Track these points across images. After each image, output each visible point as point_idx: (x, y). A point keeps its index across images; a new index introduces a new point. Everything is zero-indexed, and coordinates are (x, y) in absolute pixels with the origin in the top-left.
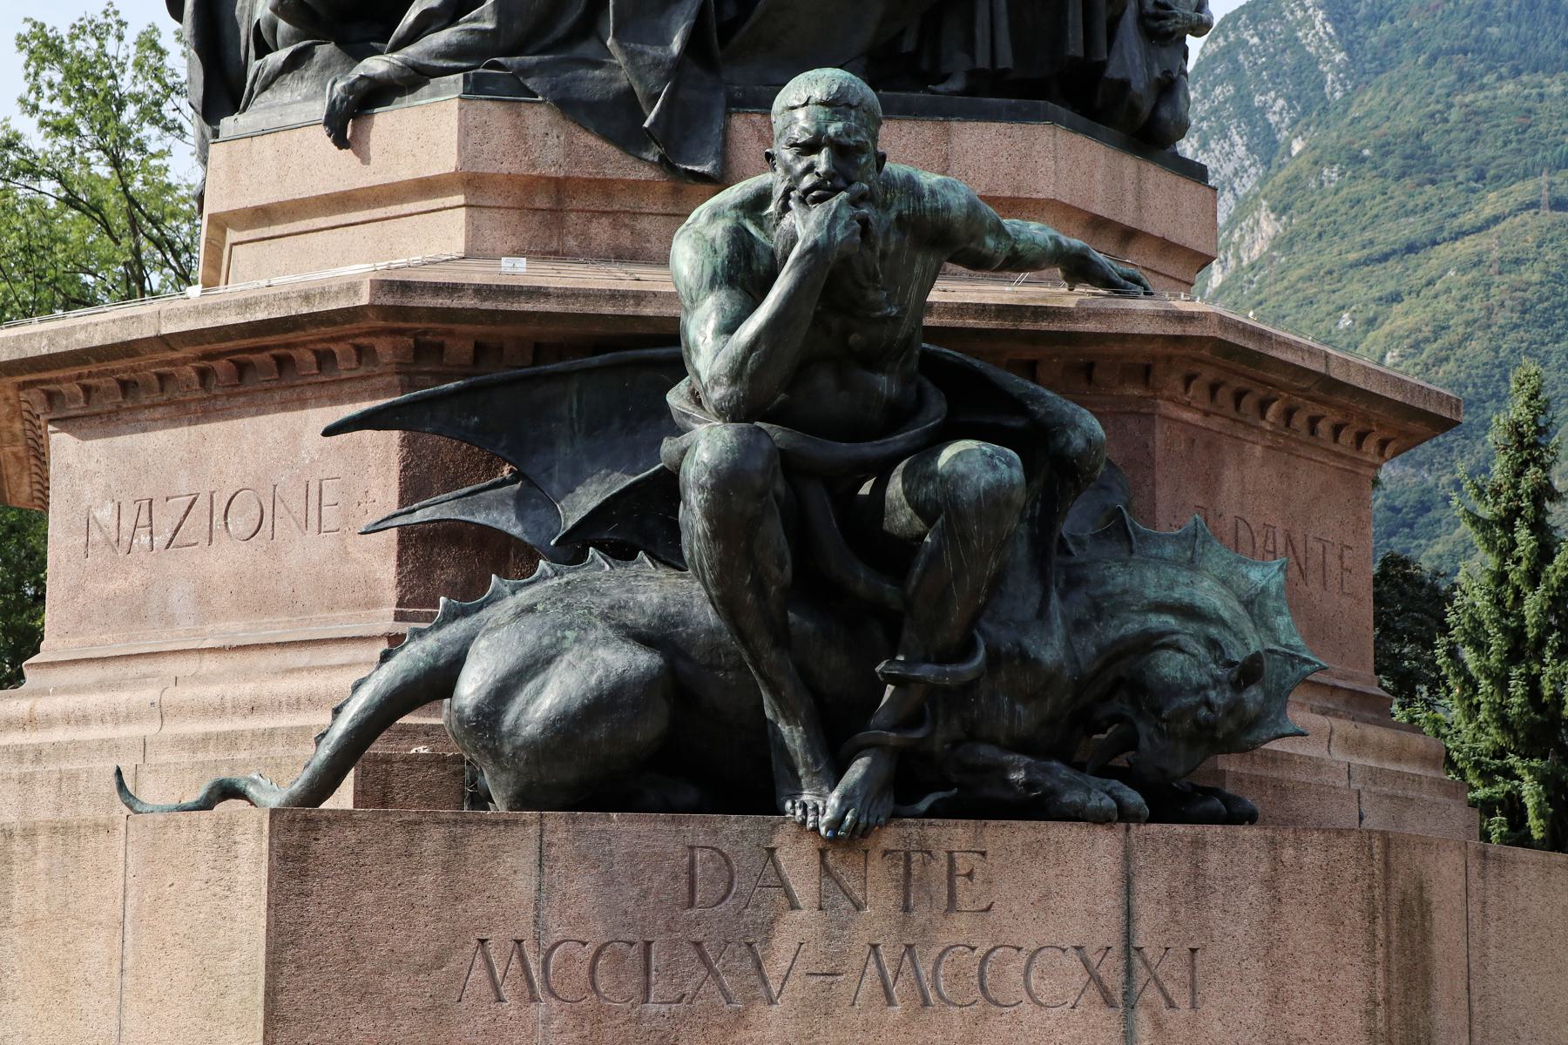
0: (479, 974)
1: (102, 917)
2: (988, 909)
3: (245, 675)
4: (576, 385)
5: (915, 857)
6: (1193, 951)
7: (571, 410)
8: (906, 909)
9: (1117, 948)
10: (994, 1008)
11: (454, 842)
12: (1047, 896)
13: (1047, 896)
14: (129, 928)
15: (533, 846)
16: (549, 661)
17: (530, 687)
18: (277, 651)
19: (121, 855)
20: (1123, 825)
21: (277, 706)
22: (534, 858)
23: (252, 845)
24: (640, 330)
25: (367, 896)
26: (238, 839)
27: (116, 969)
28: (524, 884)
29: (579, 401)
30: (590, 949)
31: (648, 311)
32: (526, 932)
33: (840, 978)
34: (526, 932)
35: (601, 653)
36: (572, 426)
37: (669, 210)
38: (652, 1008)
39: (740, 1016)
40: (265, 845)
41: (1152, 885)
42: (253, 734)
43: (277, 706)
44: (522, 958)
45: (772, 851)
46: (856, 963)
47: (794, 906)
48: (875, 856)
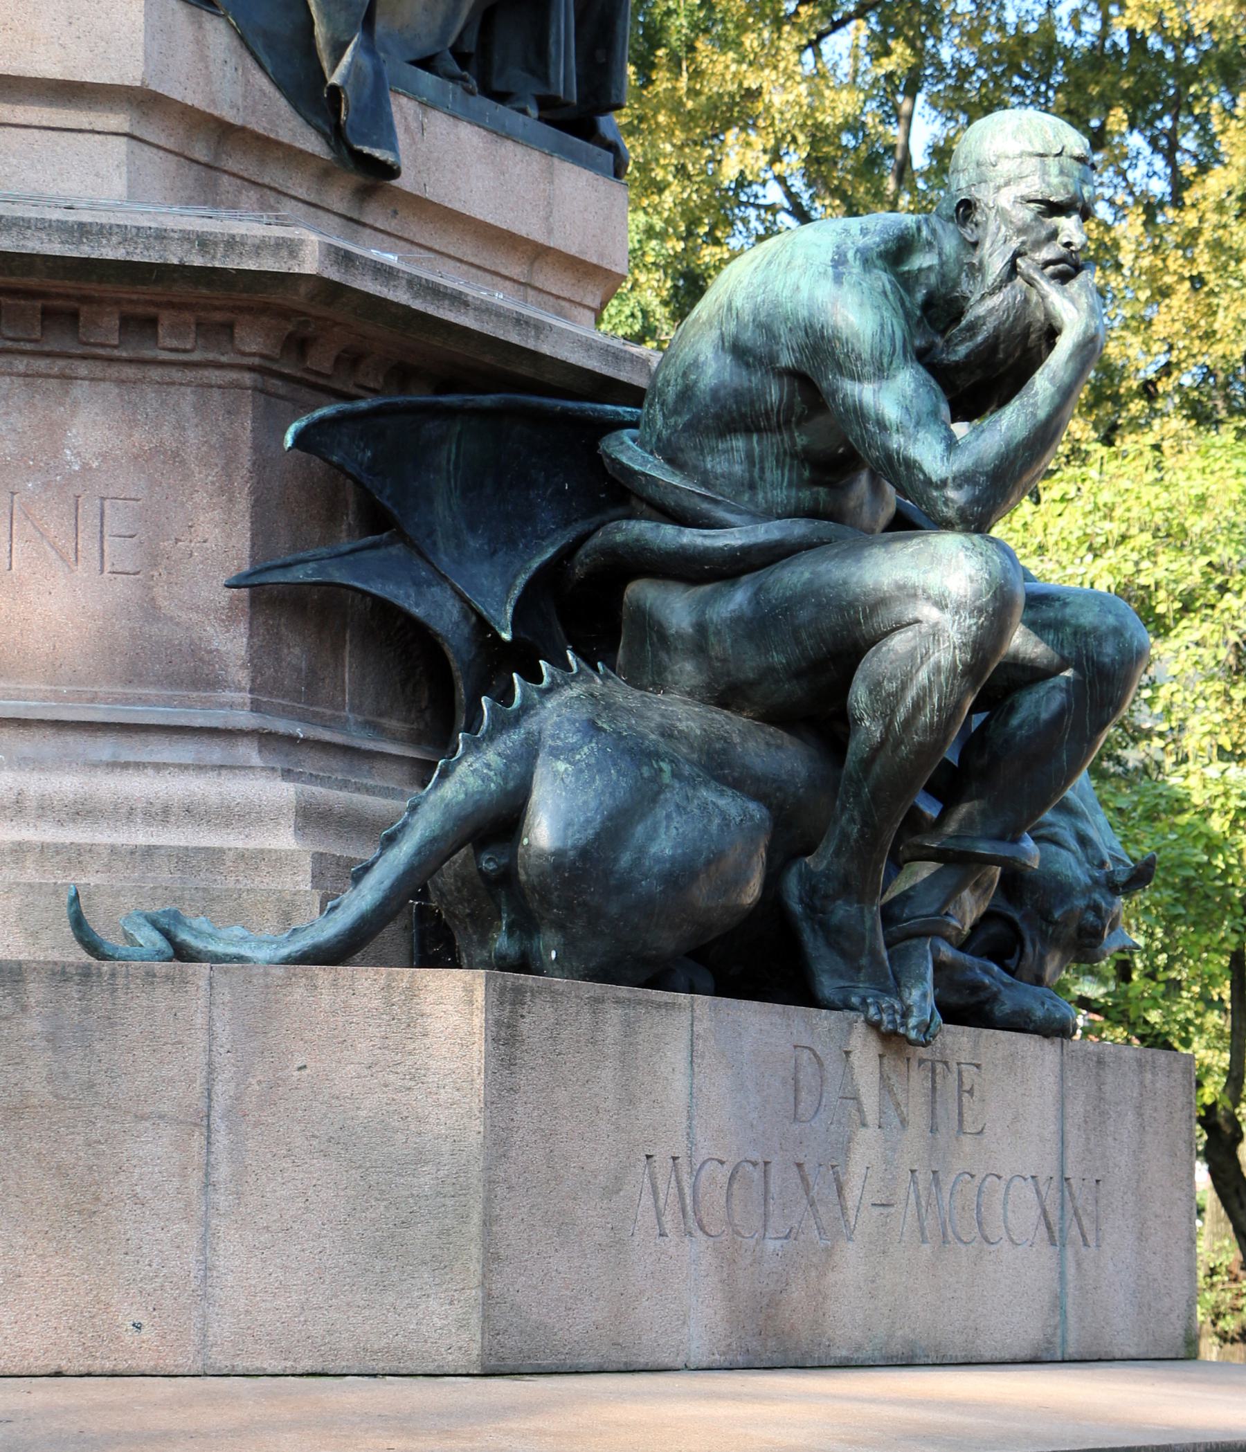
0: (647, 1200)
1: (165, 1108)
2: (980, 1133)
3: (63, 763)
4: (458, 428)
5: (939, 1067)
6: (1097, 1181)
7: (449, 461)
8: (933, 1129)
9: (1056, 1178)
10: (986, 1245)
11: (629, 1027)
12: (1015, 1119)
13: (1015, 1119)
14: (218, 1123)
15: (686, 1036)
16: (654, 800)
17: (640, 830)
18: (48, 732)
19: (200, 1020)
20: (1059, 1039)
21: (126, 813)
22: (685, 1053)
23: (455, 1019)
24: (524, 370)
25: (562, 1096)
26: (428, 1010)
27: (195, 1180)
28: (680, 1083)
29: (458, 448)
30: (727, 1170)
31: (546, 349)
32: (680, 1151)
33: (892, 1210)
34: (680, 1150)
35: (705, 793)
36: (449, 481)
37: (312, 198)
38: (771, 1245)
39: (829, 1252)
40: (478, 1020)
41: (1077, 1108)
42: (113, 850)
43: (126, 813)
44: (678, 1182)
45: (848, 1053)
46: (901, 1193)
47: (864, 1125)
48: (914, 1063)
